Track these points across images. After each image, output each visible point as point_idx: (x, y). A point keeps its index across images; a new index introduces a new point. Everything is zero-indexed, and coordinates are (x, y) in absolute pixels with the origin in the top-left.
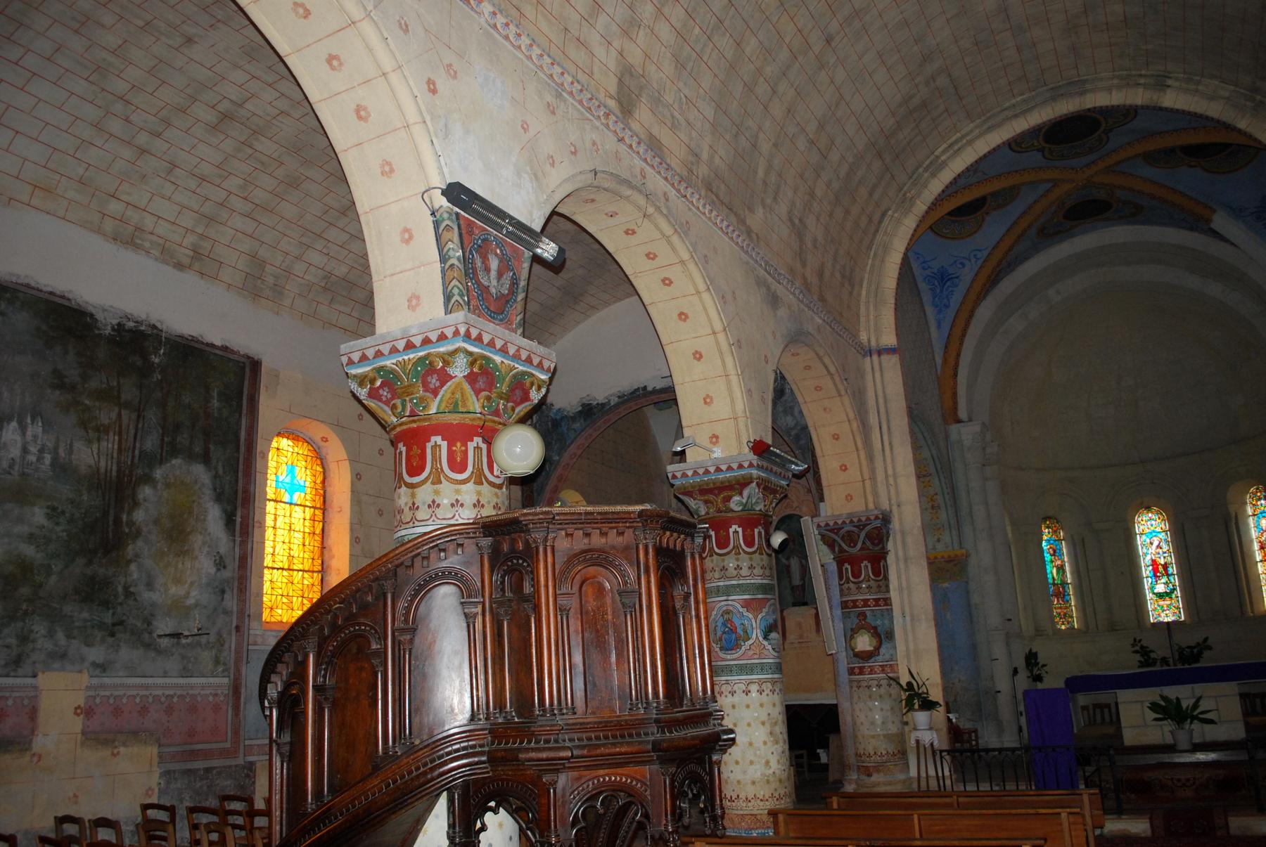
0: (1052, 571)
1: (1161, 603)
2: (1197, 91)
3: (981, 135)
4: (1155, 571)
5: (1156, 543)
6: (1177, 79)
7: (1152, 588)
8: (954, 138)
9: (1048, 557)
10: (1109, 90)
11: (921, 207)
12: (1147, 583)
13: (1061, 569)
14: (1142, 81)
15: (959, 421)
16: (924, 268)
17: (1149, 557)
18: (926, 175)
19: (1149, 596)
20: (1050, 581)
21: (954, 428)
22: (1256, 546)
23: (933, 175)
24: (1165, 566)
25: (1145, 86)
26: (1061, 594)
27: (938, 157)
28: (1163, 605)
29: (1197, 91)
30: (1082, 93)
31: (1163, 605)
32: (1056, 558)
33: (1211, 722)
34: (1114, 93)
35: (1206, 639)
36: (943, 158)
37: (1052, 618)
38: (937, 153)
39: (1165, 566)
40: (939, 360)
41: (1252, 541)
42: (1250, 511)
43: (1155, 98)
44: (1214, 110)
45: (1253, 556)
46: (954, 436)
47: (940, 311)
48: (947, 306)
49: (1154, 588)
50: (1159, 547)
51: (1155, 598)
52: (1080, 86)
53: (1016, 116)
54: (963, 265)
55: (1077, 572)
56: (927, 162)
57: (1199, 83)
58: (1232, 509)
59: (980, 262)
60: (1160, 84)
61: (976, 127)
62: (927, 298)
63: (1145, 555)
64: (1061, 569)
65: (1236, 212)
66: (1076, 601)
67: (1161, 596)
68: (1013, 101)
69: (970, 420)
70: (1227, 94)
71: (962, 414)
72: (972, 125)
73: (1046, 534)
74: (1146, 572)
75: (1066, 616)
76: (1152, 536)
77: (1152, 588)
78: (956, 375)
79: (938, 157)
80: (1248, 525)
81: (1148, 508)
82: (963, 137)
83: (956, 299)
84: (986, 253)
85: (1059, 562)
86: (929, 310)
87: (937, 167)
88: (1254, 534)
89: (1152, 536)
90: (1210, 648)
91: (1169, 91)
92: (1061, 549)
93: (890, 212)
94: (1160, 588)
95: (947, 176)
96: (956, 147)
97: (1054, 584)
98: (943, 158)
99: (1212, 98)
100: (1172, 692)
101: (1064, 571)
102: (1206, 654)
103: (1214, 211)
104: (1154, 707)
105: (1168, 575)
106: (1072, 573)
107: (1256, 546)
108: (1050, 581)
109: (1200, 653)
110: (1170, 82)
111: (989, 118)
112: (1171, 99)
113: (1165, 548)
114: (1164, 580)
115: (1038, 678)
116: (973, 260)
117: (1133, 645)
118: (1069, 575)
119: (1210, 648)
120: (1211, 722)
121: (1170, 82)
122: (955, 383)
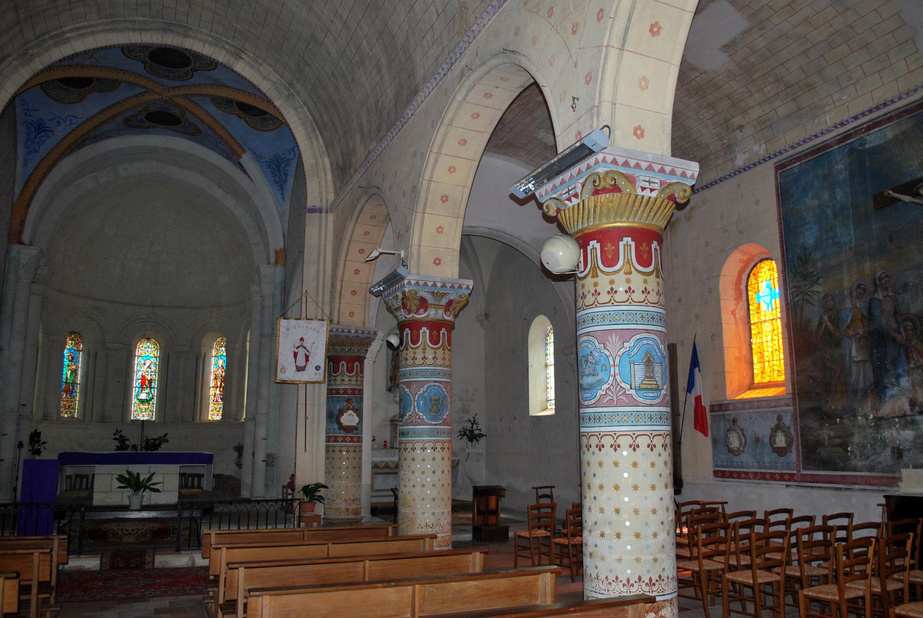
0: (67, 372)
1: (142, 406)
2: (258, 69)
3: (103, 31)
4: (143, 383)
5: (148, 364)
6: (248, 56)
7: (137, 395)
8: (82, 24)
9: (66, 362)
10: (204, 42)
11: (38, 65)
12: (134, 392)
13: (74, 372)
14: (227, 47)
15: (21, 243)
16: (25, 114)
17: (140, 373)
18: (50, 42)
19: (134, 400)
20: (64, 380)
21: (16, 247)
22: (212, 377)
23: (56, 45)
24: (150, 382)
25: (228, 52)
26: (70, 391)
27: (64, 33)
28: (142, 408)
29: (258, 69)
30: (186, 36)
31: (142, 408)
32: (73, 363)
33: (157, 491)
34: (207, 45)
35: (166, 435)
36: (68, 35)
37: (59, 407)
38: (65, 29)
39: (150, 382)
40: (17, 191)
42: (214, 353)
43: (232, 61)
44: (265, 86)
45: (208, 383)
46: (13, 254)
47: (30, 152)
48: (36, 151)
49: (138, 394)
50: (149, 367)
51: (137, 402)
52: (185, 30)
53: (134, 30)
54: (59, 124)
55: (86, 376)
56: (54, 33)
57: (260, 65)
58: (203, 349)
59: (73, 127)
60: (237, 54)
61: (101, 24)
62: (21, 138)
63: (138, 371)
64: (74, 372)
65: (258, 157)
66: (80, 397)
67: (142, 402)
68: (136, 18)
69: (31, 244)
70: (275, 80)
71: (26, 238)
72: (99, 21)
73: (69, 345)
74: (136, 383)
75: (70, 408)
76: (146, 359)
77: (137, 395)
78: (28, 206)
79: (64, 33)
81: (148, 339)
82: (89, 26)
83: (44, 149)
84: (80, 121)
85: (74, 367)
86: (21, 150)
87: (60, 39)
88: (213, 368)
89: (146, 359)
90: (167, 441)
91: (241, 61)
92: (78, 358)
93: (10, 59)
94: (143, 396)
95: (66, 50)
96: (81, 32)
97: (66, 383)
98: (68, 35)
99: (265, 78)
100: (135, 468)
101: (76, 374)
102: (164, 445)
103: (245, 152)
104: (121, 478)
105: (151, 388)
106: (82, 377)
107: (212, 377)
108: (64, 380)
109: (160, 444)
110: (243, 56)
111: (113, 22)
112: (241, 67)
113: (153, 368)
114: (148, 390)
115: (38, 452)
116: (68, 122)
117: (115, 434)
119: (167, 441)
120: (157, 491)
121: (243, 56)
122: (26, 213)
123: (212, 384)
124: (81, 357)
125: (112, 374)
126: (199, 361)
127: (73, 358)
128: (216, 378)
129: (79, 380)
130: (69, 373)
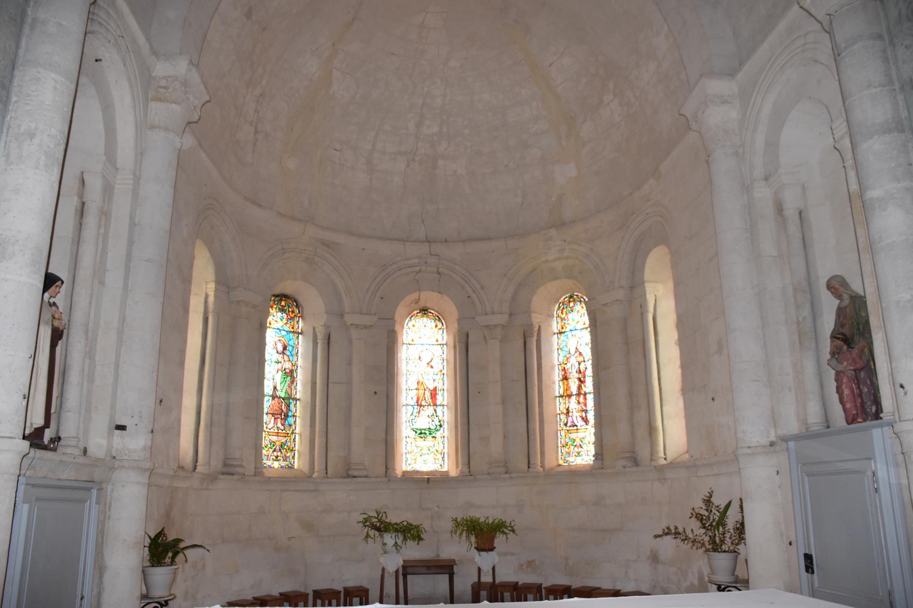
0: (273, 377)
1: (420, 442)
5: (426, 359)
9: (271, 354)
22: (557, 375)
28: (424, 446)
37: (258, 448)
41: (553, 368)
49: (410, 419)
58: (536, 319)
64: (290, 374)
66: (303, 426)
67: (421, 433)
73: (276, 321)
80: (551, 345)
85: (288, 365)
94: (423, 422)
97: (274, 397)
118: (299, 387)
123: (558, 389)
124: (302, 345)
125: (360, 381)
126: (527, 341)
127: (285, 348)
128: (565, 378)
129: (300, 390)
130: (279, 377)
